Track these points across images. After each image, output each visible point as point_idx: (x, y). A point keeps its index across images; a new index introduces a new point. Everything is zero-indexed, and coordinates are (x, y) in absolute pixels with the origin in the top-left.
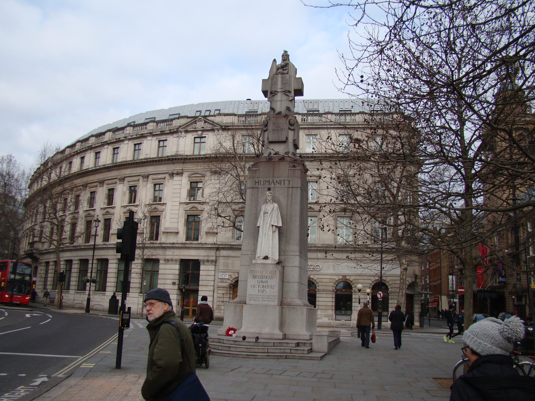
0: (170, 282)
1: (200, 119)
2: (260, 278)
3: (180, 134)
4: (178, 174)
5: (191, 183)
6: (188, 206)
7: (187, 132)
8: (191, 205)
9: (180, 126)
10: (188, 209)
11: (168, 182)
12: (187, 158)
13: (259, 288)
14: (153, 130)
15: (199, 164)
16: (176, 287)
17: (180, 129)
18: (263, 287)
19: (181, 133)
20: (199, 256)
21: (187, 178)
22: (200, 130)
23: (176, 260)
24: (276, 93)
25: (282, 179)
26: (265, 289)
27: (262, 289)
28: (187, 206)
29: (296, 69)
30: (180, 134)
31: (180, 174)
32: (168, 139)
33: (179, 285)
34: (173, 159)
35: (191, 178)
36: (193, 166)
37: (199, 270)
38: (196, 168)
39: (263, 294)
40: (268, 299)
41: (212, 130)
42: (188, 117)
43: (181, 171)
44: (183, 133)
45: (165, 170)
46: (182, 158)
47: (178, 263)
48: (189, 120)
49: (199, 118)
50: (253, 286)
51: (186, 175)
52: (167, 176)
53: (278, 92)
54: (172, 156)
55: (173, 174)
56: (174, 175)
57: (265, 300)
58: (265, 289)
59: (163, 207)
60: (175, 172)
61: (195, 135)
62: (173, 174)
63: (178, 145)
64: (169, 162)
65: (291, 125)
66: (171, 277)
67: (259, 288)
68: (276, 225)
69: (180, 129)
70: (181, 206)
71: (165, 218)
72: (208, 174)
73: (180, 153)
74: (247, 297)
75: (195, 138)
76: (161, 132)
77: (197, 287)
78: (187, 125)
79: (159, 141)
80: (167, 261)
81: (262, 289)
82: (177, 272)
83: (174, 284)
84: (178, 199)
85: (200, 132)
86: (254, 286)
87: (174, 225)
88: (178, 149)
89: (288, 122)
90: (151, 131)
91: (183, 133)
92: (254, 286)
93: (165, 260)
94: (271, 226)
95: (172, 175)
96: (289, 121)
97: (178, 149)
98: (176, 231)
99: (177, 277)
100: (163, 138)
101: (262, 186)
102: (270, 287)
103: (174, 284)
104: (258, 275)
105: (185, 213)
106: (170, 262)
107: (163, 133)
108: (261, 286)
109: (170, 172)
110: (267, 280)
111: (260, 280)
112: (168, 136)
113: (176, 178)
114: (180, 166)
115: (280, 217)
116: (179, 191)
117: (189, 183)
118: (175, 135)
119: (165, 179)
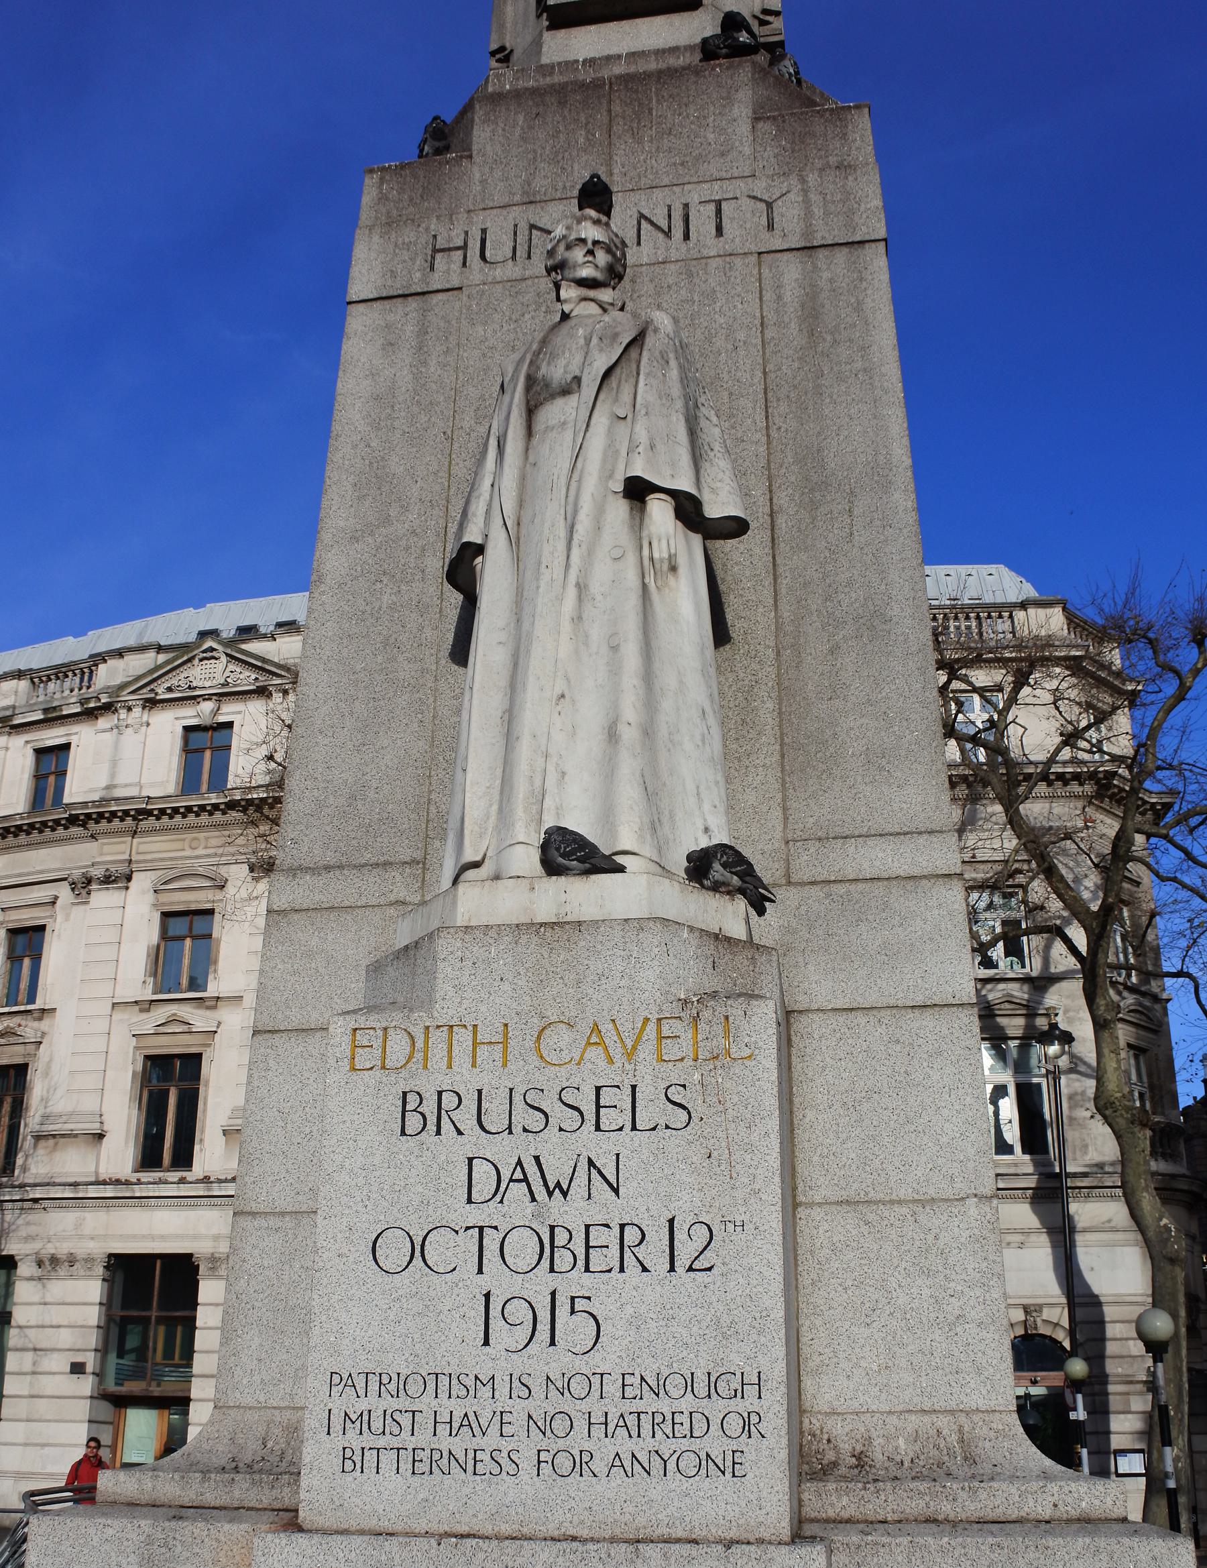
0: (61, 1363)
1: (212, 649)
2: (495, 1118)
3: (123, 713)
4: (108, 880)
5: (166, 915)
6: (151, 1014)
7: (152, 703)
8: (161, 1014)
9: (122, 687)
10: (149, 1028)
11: (67, 919)
12: (149, 813)
13: (497, 1279)
14: (14, 707)
15: (202, 835)
16: (86, 1385)
17: (125, 696)
18: (547, 1249)
19: (129, 709)
20: (196, 1237)
21: (150, 897)
22: (208, 698)
23: (89, 1260)
25: (694, 198)
26: (574, 1282)
27: (539, 1286)
28: (144, 1016)
30: (123, 713)
31: (119, 879)
32: (74, 740)
33: (99, 1375)
34: (89, 816)
35: (164, 898)
36: (178, 845)
37: (193, 1304)
38: (188, 853)
39: (558, 1362)
40: (632, 1424)
41: (262, 692)
42: (160, 649)
43: (123, 869)
44: (137, 711)
45: (58, 866)
46: (126, 813)
47: (100, 1270)
48: (162, 658)
49: (205, 646)
50: (395, 1251)
51: (142, 883)
52: (64, 892)
54: (85, 804)
55: (89, 881)
56: (94, 886)
57: (581, 1463)
58: (574, 1282)
59: (44, 1025)
60: (98, 872)
61: (190, 715)
62: (89, 881)
63: (114, 763)
64: (75, 830)
66: (65, 1338)
67: (497, 1279)
68: (684, 484)
69: (125, 696)
70: (117, 1016)
71: (46, 1074)
72: (238, 873)
73: (119, 793)
74: (313, 1421)
75: (187, 729)
76: (45, 711)
77: (184, 1385)
78: (154, 676)
79: (40, 752)
80: (50, 1264)
81: (539, 1286)
82: (93, 1316)
83: (77, 1369)
84: (105, 990)
85: (207, 707)
86: (418, 1250)
87: (89, 1104)
88: (113, 775)
90: (8, 713)
91: (137, 711)
92: (418, 1250)
93: (40, 1264)
94: (620, 508)
95: (83, 885)
97: (113, 775)
98: (95, 1128)
99: (93, 1339)
100: (52, 736)
101: (498, 273)
102: (655, 1252)
103: (77, 1369)
104: (466, 1080)
105: (136, 1048)
106: (63, 1271)
107: (53, 717)
108: (523, 1248)
109: (76, 874)
110: (602, 1148)
111: (505, 1151)
112: (75, 728)
113: (102, 898)
114: (122, 847)
116: (109, 953)
117: (157, 917)
118: (103, 722)
119: (54, 903)
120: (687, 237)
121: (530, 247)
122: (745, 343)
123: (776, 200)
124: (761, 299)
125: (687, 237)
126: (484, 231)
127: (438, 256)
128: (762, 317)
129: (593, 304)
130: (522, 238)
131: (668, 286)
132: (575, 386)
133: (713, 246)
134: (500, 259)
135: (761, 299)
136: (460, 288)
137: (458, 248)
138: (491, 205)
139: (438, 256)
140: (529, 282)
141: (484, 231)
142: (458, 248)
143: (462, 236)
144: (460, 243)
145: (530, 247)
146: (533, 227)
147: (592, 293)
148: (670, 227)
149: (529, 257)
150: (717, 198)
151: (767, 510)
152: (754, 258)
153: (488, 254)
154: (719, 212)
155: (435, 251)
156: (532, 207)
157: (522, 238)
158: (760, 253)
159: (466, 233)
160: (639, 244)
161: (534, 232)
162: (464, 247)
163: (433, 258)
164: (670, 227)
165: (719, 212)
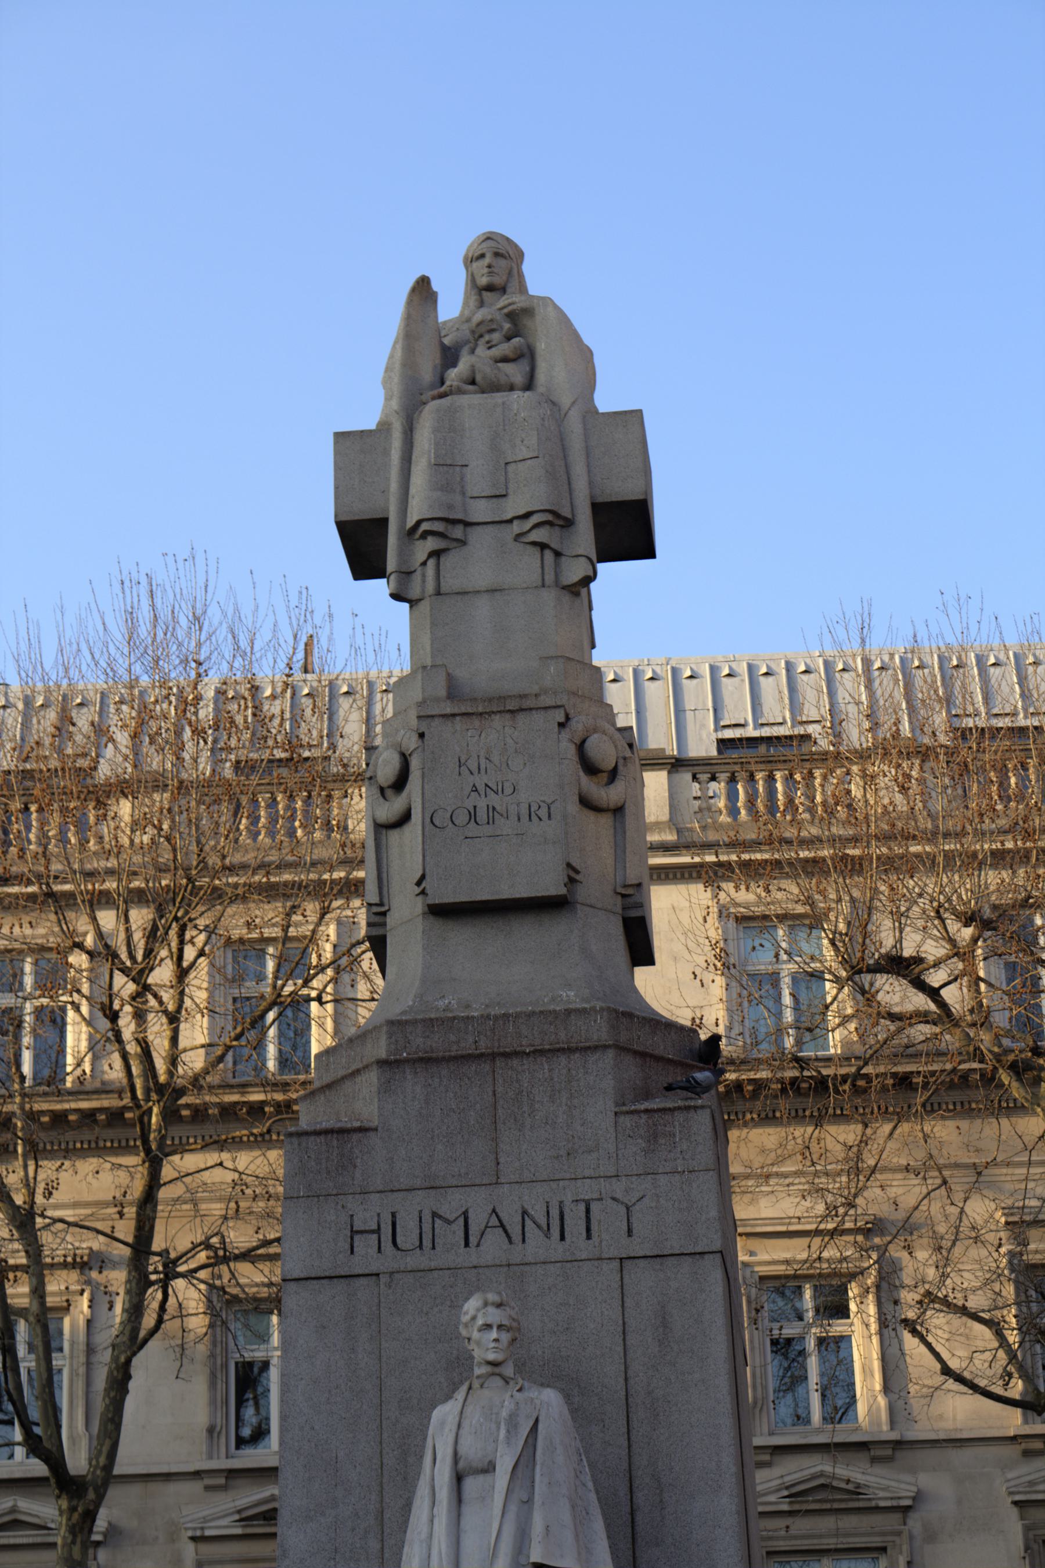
24: (458, 532)
25: (568, 1198)
29: (587, 355)
53: (467, 524)
65: (590, 768)
89: (571, 751)
96: (581, 747)
115: (593, 1496)
120: (562, 1238)
121: (433, 1236)
122: (611, 1349)
123: (634, 1204)
124: (623, 1306)
125: (562, 1238)
126: (394, 1215)
127: (357, 1238)
128: (624, 1323)
129: (498, 1378)
130: (427, 1227)
131: (549, 1289)
132: (491, 1469)
133: (584, 1249)
134: (409, 1246)
135: (623, 1306)
136: (378, 1275)
137: (372, 1232)
138: (398, 1187)
139: (357, 1238)
140: (435, 1274)
141: (394, 1215)
142: (372, 1232)
143: (375, 1220)
144: (375, 1227)
145: (433, 1236)
146: (435, 1215)
147: (497, 1370)
148: (548, 1225)
149: (434, 1248)
150: (587, 1198)
151: (628, 1509)
152: (616, 1264)
153: (399, 1240)
154: (588, 1211)
155: (354, 1233)
156: (432, 1192)
157: (427, 1227)
158: (621, 1259)
159: (379, 1215)
160: (524, 1241)
161: (438, 1221)
162: (378, 1231)
163: (352, 1238)
164: (548, 1225)
165: (588, 1211)
